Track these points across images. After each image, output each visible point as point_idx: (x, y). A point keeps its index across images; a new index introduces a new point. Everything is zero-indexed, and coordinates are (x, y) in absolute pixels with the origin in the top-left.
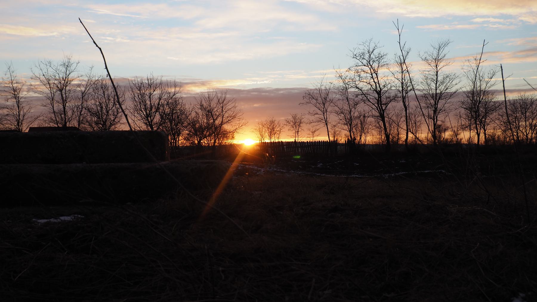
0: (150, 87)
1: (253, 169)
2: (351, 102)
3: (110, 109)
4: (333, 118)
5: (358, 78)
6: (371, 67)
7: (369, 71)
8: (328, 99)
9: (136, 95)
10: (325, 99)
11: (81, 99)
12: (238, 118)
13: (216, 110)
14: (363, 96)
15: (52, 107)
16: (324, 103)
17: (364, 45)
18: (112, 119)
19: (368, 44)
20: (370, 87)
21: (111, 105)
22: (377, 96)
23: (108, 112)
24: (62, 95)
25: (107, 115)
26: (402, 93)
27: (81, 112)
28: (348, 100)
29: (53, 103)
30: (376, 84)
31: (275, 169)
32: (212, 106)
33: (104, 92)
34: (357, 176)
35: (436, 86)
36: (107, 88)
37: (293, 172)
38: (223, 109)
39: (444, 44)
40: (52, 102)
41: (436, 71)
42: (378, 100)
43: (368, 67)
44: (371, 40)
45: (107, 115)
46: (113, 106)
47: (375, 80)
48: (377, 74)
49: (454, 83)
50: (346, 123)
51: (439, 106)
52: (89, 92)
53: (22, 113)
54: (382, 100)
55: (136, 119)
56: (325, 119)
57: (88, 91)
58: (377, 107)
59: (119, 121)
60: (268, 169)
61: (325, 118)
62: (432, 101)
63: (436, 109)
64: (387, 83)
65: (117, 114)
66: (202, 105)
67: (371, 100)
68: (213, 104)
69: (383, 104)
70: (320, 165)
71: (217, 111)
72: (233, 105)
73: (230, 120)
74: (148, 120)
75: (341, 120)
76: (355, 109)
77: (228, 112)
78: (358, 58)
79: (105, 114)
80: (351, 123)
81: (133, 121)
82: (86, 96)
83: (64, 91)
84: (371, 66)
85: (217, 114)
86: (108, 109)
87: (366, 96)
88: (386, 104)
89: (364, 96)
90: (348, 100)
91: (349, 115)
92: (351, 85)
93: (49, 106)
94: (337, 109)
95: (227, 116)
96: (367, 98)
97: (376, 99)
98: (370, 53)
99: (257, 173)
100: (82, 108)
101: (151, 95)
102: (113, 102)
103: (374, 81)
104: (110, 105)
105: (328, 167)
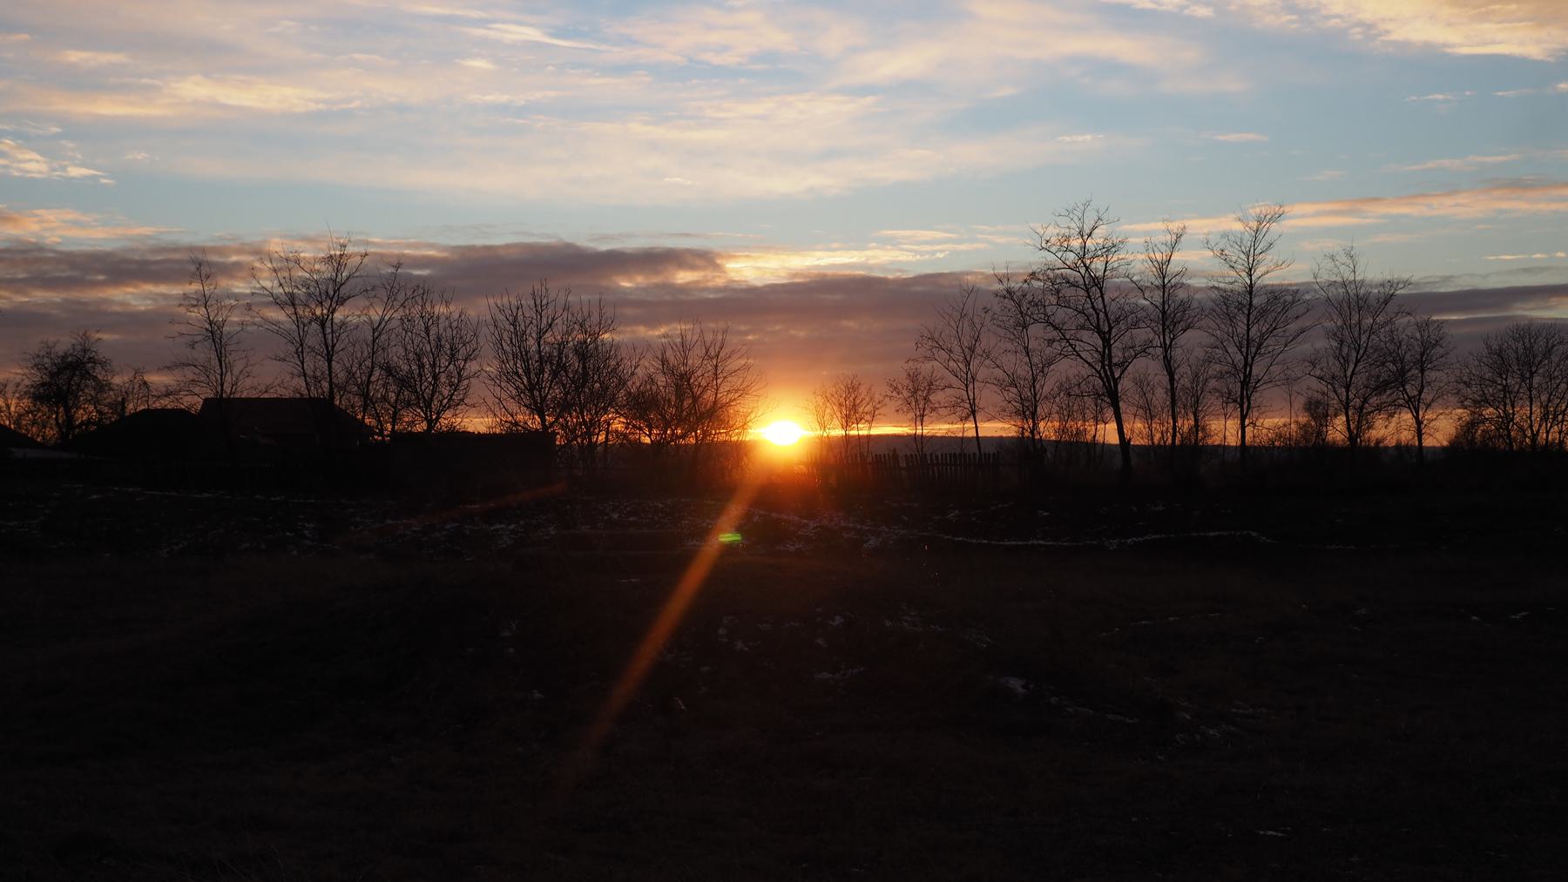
2: (1035, 360)
3: (442, 370)
4: (988, 396)
5: (1053, 300)
6: (1087, 270)
8: (978, 351)
10: (972, 350)
11: (371, 346)
12: (754, 393)
13: (699, 373)
14: (1063, 344)
15: (299, 363)
16: (968, 359)
17: (1071, 215)
18: (446, 393)
19: (1080, 215)
20: (1082, 320)
21: (444, 363)
22: (1100, 342)
23: (436, 377)
24: (325, 335)
25: (435, 386)
26: (1161, 336)
27: (370, 376)
29: (302, 352)
30: (1098, 315)
31: (843, 524)
32: (690, 362)
33: (427, 330)
35: (1248, 321)
36: (435, 318)
37: (886, 530)
38: (718, 372)
39: (1269, 217)
41: (1249, 282)
42: (1103, 356)
43: (1079, 272)
44: (1087, 204)
45: (433, 385)
46: (449, 364)
47: (1095, 304)
48: (1101, 289)
49: (1290, 314)
51: (1257, 370)
53: (228, 378)
54: (1113, 354)
55: (504, 396)
56: (970, 400)
58: (1099, 372)
59: (463, 400)
60: (825, 522)
61: (971, 397)
62: (1239, 358)
63: (1248, 376)
64: (1127, 308)
65: (459, 382)
66: (664, 361)
67: (1083, 355)
68: (694, 360)
69: (1116, 364)
71: (701, 378)
72: (743, 362)
73: (735, 399)
75: (1010, 402)
76: (1045, 375)
77: (729, 379)
79: (430, 383)
80: (1036, 407)
82: (384, 337)
83: (328, 324)
84: (1087, 269)
85: (704, 383)
86: (437, 371)
88: (1124, 365)
91: (1030, 390)
92: (1035, 316)
93: (292, 360)
94: (998, 373)
95: (728, 389)
96: (1074, 349)
97: (1097, 351)
100: (373, 367)
101: (540, 338)
102: (448, 352)
103: (1093, 307)
104: (442, 361)
105: (974, 519)
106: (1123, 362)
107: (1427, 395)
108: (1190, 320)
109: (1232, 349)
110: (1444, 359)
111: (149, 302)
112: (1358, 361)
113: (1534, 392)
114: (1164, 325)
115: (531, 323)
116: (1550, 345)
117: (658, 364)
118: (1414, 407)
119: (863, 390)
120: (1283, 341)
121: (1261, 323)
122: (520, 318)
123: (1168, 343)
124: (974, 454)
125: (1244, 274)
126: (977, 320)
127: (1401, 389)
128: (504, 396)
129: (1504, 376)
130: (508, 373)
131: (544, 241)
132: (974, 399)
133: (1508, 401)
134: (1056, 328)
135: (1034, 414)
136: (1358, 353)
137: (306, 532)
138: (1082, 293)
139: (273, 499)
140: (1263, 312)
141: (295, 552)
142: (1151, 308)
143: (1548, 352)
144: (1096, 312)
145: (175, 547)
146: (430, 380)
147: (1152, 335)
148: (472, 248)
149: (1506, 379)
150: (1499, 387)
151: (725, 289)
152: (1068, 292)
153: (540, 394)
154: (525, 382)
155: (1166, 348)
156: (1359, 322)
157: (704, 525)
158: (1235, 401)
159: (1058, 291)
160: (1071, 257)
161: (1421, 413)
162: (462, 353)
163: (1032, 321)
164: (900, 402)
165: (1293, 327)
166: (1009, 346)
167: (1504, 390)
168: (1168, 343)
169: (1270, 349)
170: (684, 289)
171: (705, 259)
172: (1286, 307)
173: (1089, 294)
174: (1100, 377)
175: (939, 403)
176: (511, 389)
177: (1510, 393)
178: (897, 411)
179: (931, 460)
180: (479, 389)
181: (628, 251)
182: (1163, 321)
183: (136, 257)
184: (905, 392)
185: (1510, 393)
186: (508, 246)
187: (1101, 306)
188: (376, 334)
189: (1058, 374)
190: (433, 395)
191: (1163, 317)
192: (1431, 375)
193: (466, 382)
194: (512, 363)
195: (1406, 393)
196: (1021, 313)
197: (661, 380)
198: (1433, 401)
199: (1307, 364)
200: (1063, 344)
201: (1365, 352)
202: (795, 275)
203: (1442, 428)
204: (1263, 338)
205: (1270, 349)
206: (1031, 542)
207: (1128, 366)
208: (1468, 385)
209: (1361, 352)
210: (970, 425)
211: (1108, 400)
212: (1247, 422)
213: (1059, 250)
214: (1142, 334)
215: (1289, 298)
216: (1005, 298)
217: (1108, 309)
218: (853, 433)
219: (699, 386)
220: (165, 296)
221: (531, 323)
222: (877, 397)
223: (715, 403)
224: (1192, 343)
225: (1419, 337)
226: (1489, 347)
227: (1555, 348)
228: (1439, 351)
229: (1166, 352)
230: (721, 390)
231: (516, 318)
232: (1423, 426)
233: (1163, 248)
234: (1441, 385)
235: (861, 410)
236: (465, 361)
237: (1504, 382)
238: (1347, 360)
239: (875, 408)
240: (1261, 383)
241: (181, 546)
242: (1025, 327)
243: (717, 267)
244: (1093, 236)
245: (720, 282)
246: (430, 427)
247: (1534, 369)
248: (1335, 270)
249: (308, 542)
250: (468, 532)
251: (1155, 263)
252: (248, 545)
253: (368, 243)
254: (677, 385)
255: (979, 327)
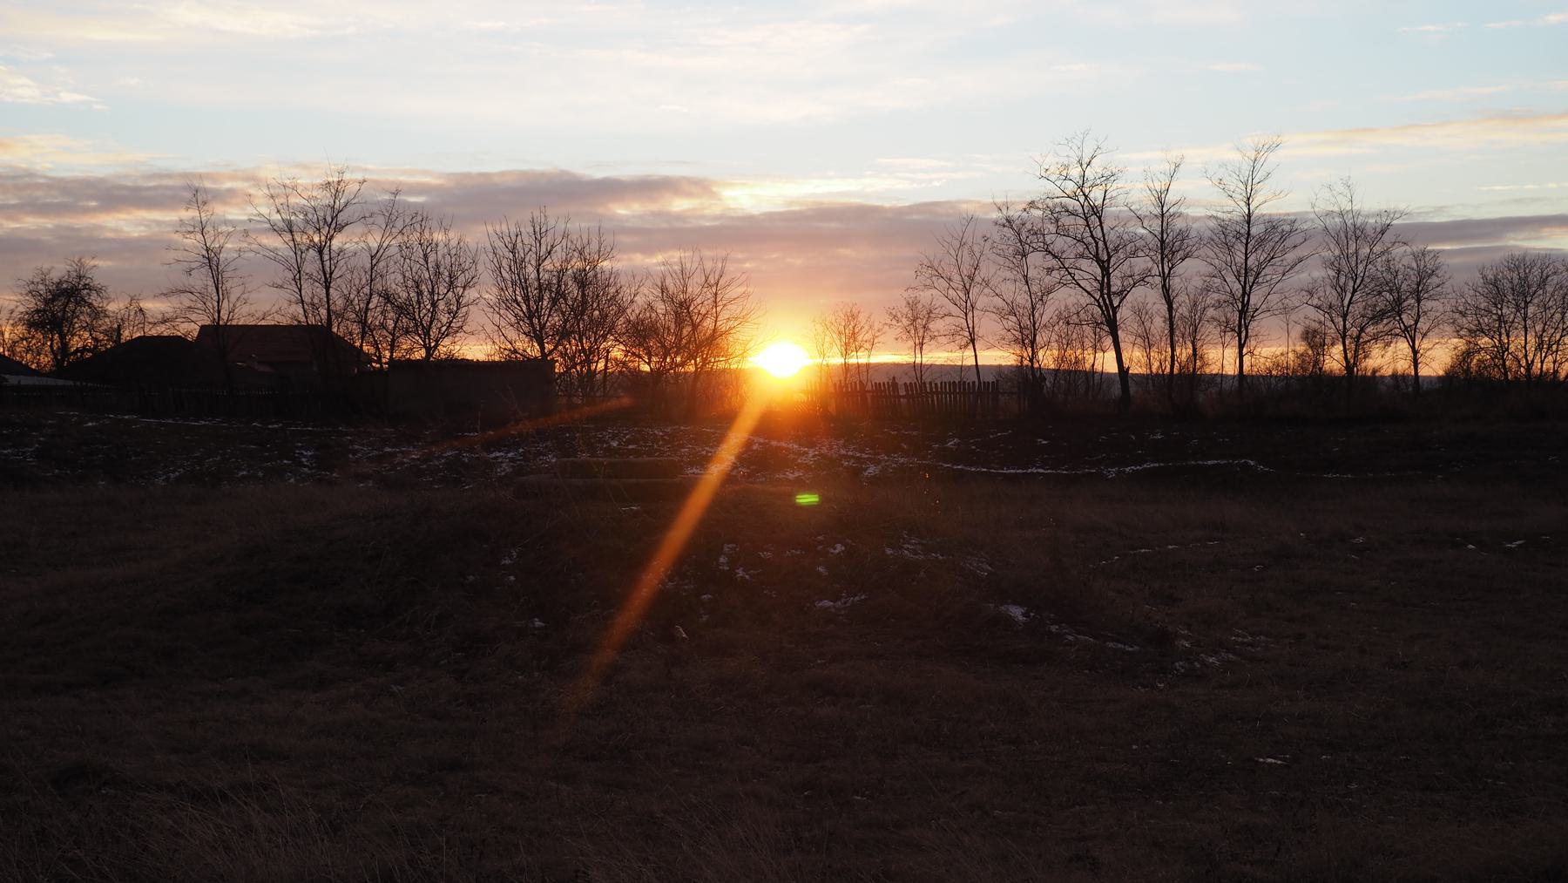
0: (538, 244)
1: (787, 449)
2: (1034, 288)
3: (441, 297)
4: (988, 325)
7: (1081, 211)
8: (978, 279)
9: (505, 263)
10: (971, 278)
13: (699, 301)
14: (1062, 273)
15: (297, 290)
16: (968, 288)
17: (1070, 144)
18: (444, 320)
19: (1079, 144)
20: (1081, 248)
21: (443, 290)
22: (1099, 271)
23: (434, 304)
24: (322, 262)
25: (434, 313)
26: (1160, 265)
27: (368, 303)
28: (1027, 282)
29: (300, 279)
30: (1097, 243)
31: (843, 452)
32: (690, 290)
33: (426, 257)
34: (1041, 471)
35: (1246, 251)
36: (433, 245)
37: (886, 458)
38: (718, 300)
39: (1267, 146)
40: (297, 277)
41: (1247, 212)
42: (1102, 285)
43: (1078, 200)
45: (432, 313)
46: (448, 291)
48: (1100, 218)
49: (1289, 243)
50: (1020, 337)
51: (1255, 299)
52: (387, 254)
53: (225, 304)
55: (503, 323)
57: (386, 253)
58: (1098, 301)
59: (461, 327)
60: (824, 450)
61: (971, 326)
62: (1237, 288)
63: (1245, 305)
64: (1126, 237)
65: (458, 309)
66: (663, 289)
67: (1081, 283)
68: (694, 288)
69: (1114, 293)
70: (952, 443)
71: (702, 304)
72: (741, 290)
74: (532, 324)
76: (1044, 304)
77: (728, 307)
78: (1053, 178)
79: (429, 310)
80: (1035, 336)
81: (496, 328)
82: (382, 264)
83: (326, 251)
85: (703, 311)
86: (436, 298)
87: (1070, 274)
88: (1123, 294)
89: (1067, 273)
90: (1027, 282)
91: (1030, 319)
92: (1034, 245)
93: (290, 287)
94: (998, 302)
97: (1096, 279)
98: (1084, 164)
99: (797, 459)
100: (371, 295)
101: (539, 265)
102: (447, 279)
103: (1092, 236)
104: (441, 288)
105: (973, 447)
106: (1122, 292)
107: (1423, 325)
108: (1189, 249)
109: (1231, 278)
110: (1439, 289)
111: (142, 228)
112: (1354, 291)
113: (1529, 322)
114: (1162, 254)
115: (530, 250)
116: (1545, 275)
117: (657, 292)
118: (1411, 337)
119: (862, 319)
120: (1281, 270)
121: (1259, 252)
122: (519, 245)
123: (1166, 271)
124: (974, 383)
125: (1243, 204)
126: (976, 248)
127: (1398, 318)
128: (503, 323)
129: (1499, 306)
130: (507, 300)
131: (539, 168)
132: (973, 328)
133: (1503, 331)
134: (1055, 257)
135: (1033, 342)
136: (1355, 284)
137: (304, 460)
138: (1082, 222)
139: (270, 426)
140: (1261, 242)
141: (292, 480)
142: (1150, 237)
143: (1543, 282)
144: (1095, 241)
145: (172, 476)
146: (428, 307)
147: (1150, 264)
148: (468, 176)
149: (1501, 309)
150: (1494, 317)
151: (721, 217)
152: (1066, 220)
153: (539, 322)
154: (524, 308)
155: (1165, 277)
156: (1357, 252)
157: (704, 453)
158: (1233, 330)
159: (1057, 220)
160: (1070, 187)
161: (1417, 343)
162: (461, 280)
163: (1031, 249)
164: (899, 330)
165: (1291, 257)
166: (1008, 274)
167: (1499, 320)
168: (1166, 271)
169: (1268, 278)
170: (680, 217)
171: (701, 186)
172: (1284, 236)
173: (1087, 223)
174: (1099, 306)
175: (939, 331)
176: (510, 316)
177: (1505, 323)
178: (897, 339)
179: (931, 388)
180: (478, 317)
181: (624, 179)
182: (1162, 249)
183: (129, 184)
184: (904, 320)
185: (1505, 323)
186: (503, 174)
187: (1100, 235)
188: (374, 262)
189: (1057, 302)
190: (431, 322)
191: (1161, 245)
192: (1427, 305)
193: (464, 309)
194: (510, 290)
195: (1403, 322)
196: (1020, 241)
197: (660, 307)
198: (1429, 330)
199: (1304, 293)
200: (1062, 273)
201: (1362, 281)
202: (792, 203)
203: (1438, 358)
204: (1260, 265)
205: (1268, 278)
206: (1030, 471)
207: (1126, 295)
208: (1463, 314)
209: (1358, 281)
210: (969, 353)
211: (1107, 329)
212: (1245, 351)
213: (1058, 179)
214: (1141, 263)
215: (1287, 228)
216: (1004, 226)
217: (1106, 238)
218: (852, 361)
219: (699, 313)
220: (159, 223)
221: (530, 250)
222: (877, 326)
223: (715, 330)
224: (1190, 273)
225: (1415, 265)
226: (1484, 277)
227: (1550, 278)
228: (1434, 280)
229: (1165, 281)
230: (720, 318)
231: (515, 246)
232: (1419, 355)
233: (1162, 177)
234: (1438, 314)
235: (860, 338)
236: (464, 288)
237: (1499, 312)
238: (1344, 290)
239: (874, 337)
240: (1259, 312)
241: (177, 473)
242: (1024, 255)
243: (713, 195)
244: (1092, 164)
245: (716, 210)
246: (429, 354)
247: (1528, 299)
248: (1333, 200)
249: (306, 470)
250: (466, 460)
251: (1154, 192)
252: (245, 473)
253: (365, 170)
254: (676, 313)
255: (978, 255)
